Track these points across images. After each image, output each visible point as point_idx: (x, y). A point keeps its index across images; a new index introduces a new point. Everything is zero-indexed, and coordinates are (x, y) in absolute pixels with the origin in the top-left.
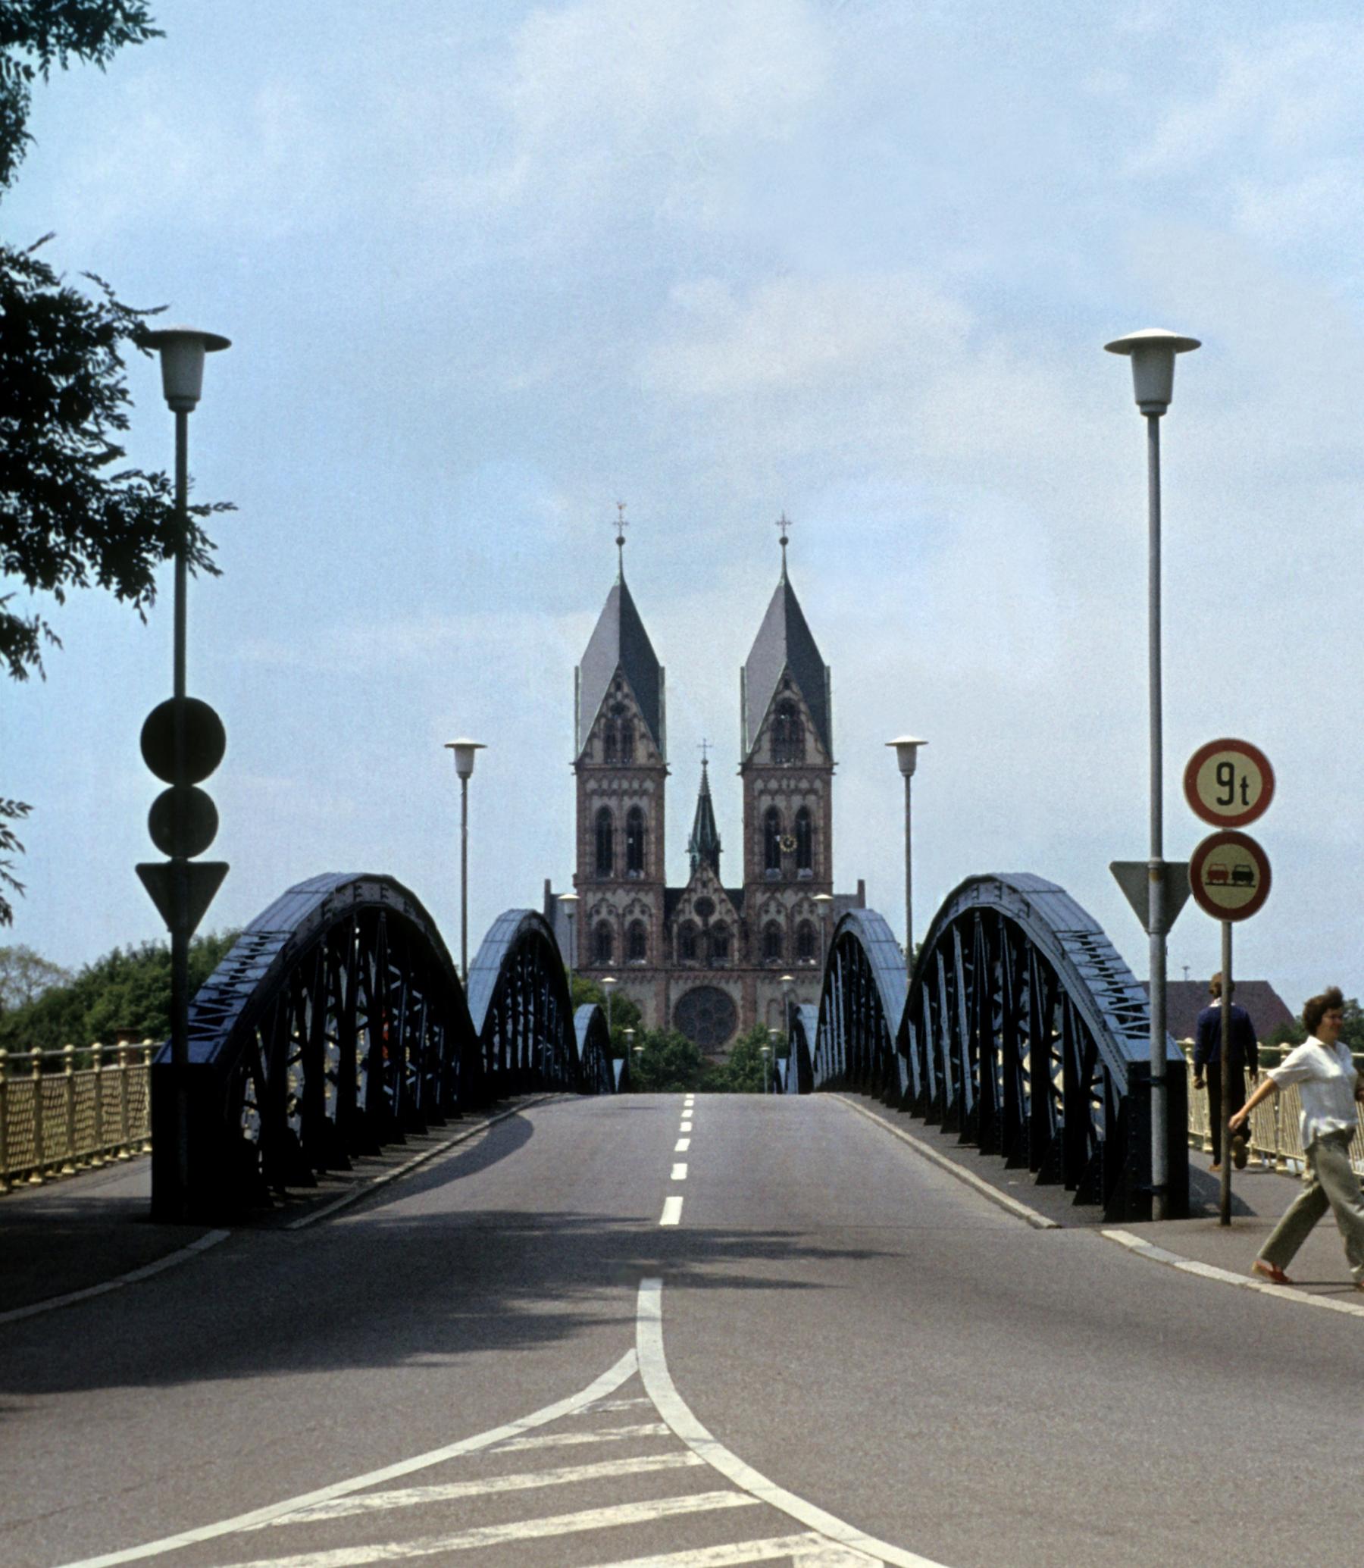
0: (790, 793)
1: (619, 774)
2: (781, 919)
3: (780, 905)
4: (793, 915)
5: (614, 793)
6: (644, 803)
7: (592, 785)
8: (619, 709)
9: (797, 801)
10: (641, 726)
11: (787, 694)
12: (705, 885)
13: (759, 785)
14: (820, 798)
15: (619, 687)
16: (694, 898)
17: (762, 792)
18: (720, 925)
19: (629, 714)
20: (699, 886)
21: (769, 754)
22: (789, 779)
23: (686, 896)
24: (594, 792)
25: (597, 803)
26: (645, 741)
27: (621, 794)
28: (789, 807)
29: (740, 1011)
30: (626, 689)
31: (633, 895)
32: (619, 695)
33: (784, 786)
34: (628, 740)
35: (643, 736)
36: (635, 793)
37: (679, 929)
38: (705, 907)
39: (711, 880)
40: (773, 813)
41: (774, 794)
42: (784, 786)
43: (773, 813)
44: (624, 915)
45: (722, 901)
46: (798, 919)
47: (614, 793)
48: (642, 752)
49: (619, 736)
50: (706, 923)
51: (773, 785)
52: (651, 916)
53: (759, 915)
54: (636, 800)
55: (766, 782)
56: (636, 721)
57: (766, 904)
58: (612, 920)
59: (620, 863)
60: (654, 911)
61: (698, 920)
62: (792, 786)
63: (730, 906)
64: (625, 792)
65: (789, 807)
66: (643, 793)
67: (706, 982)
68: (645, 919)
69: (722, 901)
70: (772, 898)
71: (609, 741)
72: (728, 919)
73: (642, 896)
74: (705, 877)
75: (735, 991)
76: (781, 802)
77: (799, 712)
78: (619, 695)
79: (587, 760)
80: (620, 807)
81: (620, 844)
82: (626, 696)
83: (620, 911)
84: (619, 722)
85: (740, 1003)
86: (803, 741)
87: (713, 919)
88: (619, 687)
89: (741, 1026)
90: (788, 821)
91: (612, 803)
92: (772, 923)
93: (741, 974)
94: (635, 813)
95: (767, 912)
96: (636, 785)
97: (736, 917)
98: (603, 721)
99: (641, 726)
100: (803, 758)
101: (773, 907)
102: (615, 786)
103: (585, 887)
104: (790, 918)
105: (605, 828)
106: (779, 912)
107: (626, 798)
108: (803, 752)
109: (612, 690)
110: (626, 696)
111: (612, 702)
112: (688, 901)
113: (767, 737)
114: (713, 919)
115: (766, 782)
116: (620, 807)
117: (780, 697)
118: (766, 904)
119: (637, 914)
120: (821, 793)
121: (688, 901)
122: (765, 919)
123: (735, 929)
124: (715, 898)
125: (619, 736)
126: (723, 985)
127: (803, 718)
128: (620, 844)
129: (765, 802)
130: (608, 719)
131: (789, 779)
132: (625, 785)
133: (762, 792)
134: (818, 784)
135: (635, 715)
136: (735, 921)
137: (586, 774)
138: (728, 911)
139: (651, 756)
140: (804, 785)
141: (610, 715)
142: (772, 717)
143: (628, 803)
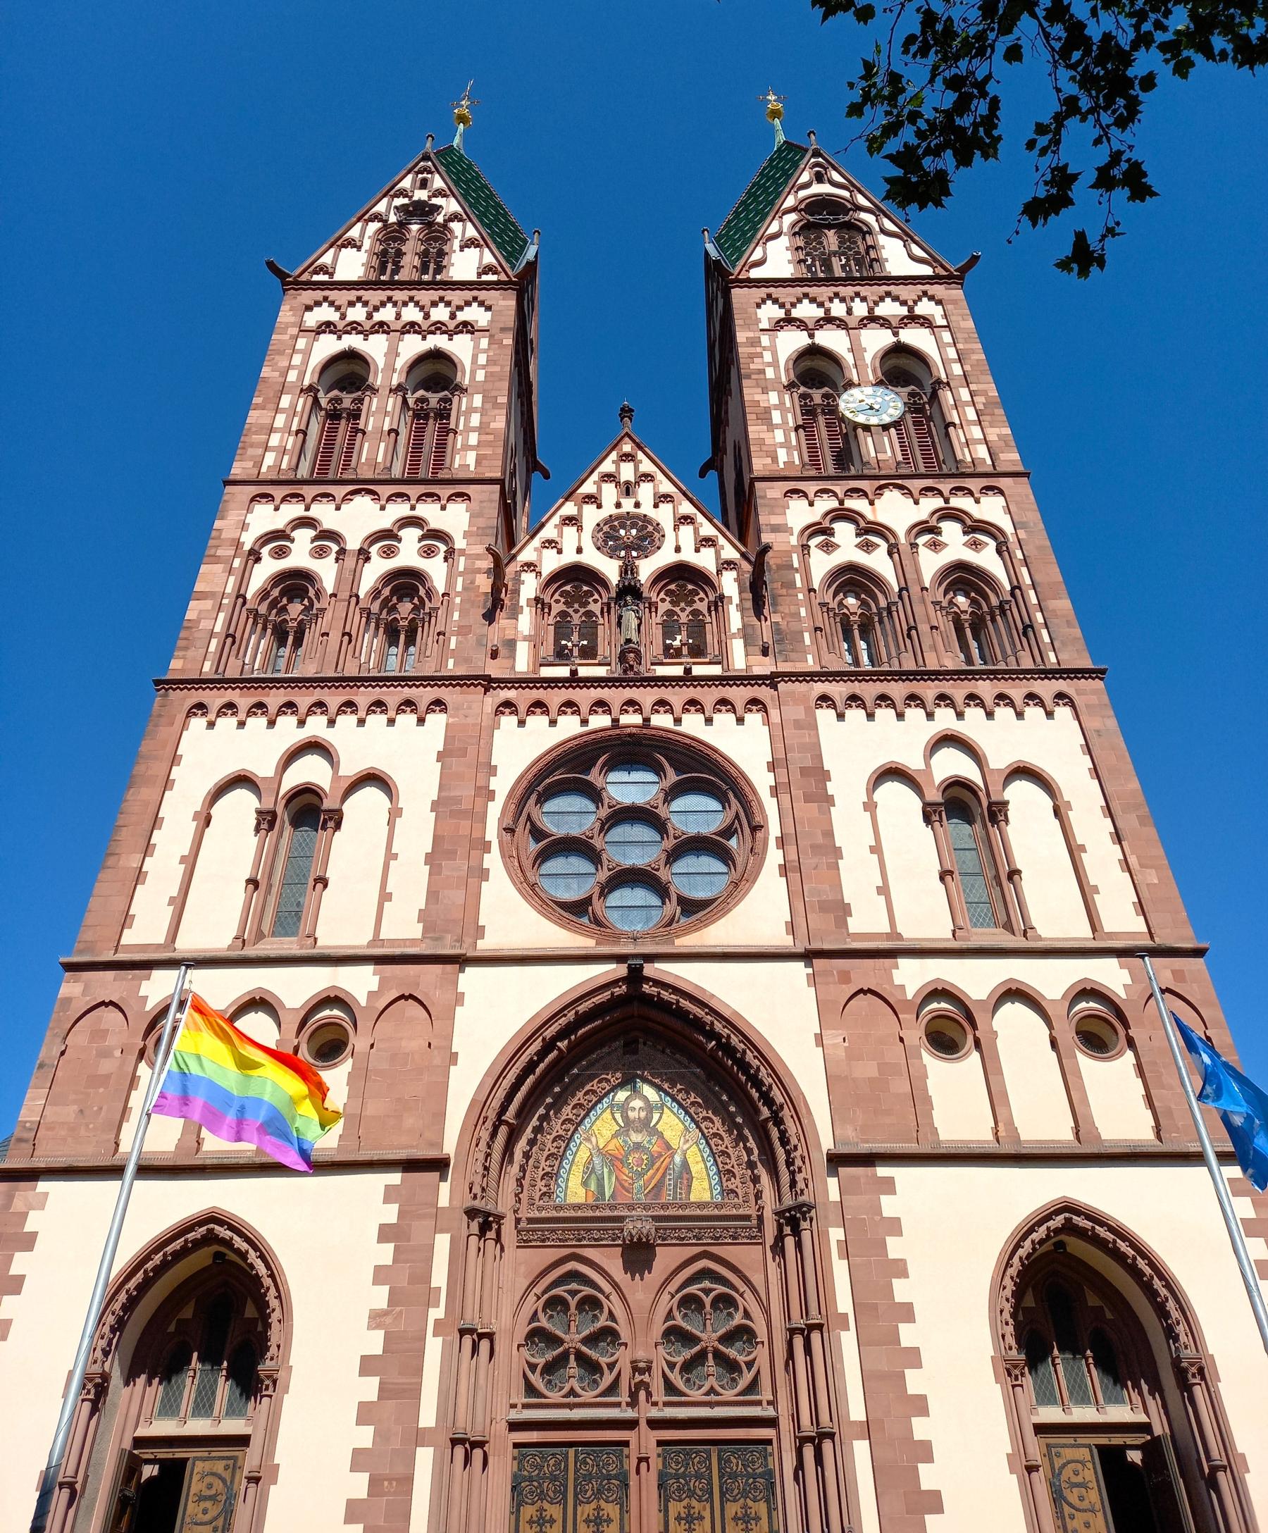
5: (382, 327)
18: (682, 576)
29: (770, 806)
46: (930, 564)
47: (382, 327)
50: (628, 569)
52: (450, 554)
60: (460, 543)
64: (412, 327)
67: (631, 719)
68: (436, 570)
73: (428, 511)
75: (743, 743)
82: (439, 193)
85: (762, 780)
87: (647, 569)
89: (774, 857)
93: (752, 692)
110: (439, 193)
119: (409, 553)
121: (570, 520)
122: (821, 564)
123: (729, 584)
126: (693, 725)
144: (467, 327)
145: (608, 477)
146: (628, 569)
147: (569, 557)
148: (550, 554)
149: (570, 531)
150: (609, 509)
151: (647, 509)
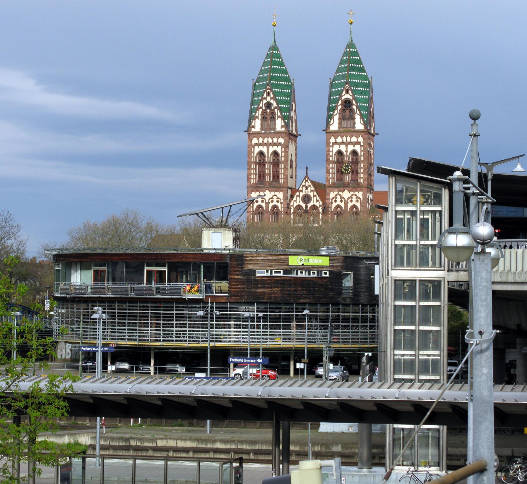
0: (347, 144)
1: (268, 135)
2: (343, 205)
3: (341, 197)
4: (348, 202)
6: (279, 149)
7: (255, 141)
8: (269, 105)
9: (351, 148)
10: (278, 113)
11: (347, 96)
12: (307, 188)
13: (333, 140)
14: (361, 146)
15: (268, 94)
16: (302, 194)
17: (335, 143)
18: (314, 207)
19: (273, 108)
20: (304, 188)
21: (337, 126)
22: (347, 137)
23: (298, 193)
24: (256, 144)
25: (257, 149)
26: (280, 119)
27: (268, 145)
28: (347, 151)
30: (272, 95)
31: (273, 193)
32: (268, 98)
33: (345, 141)
34: (273, 118)
35: (279, 117)
36: (273, 144)
37: (294, 210)
38: (307, 199)
39: (310, 186)
40: (340, 153)
41: (339, 144)
42: (345, 141)
43: (340, 153)
44: (269, 203)
45: (314, 196)
46: (350, 205)
48: (279, 125)
49: (268, 117)
50: (306, 207)
51: (339, 140)
52: (281, 203)
53: (332, 203)
54: (275, 148)
55: (336, 138)
56: (276, 110)
57: (335, 197)
58: (264, 205)
59: (269, 179)
60: (282, 201)
61: (303, 205)
62: (349, 141)
63: (318, 198)
65: (347, 151)
68: (279, 205)
69: (314, 196)
70: (338, 194)
71: (264, 119)
72: (317, 204)
73: (277, 193)
74: (307, 185)
76: (343, 148)
77: (353, 104)
78: (268, 98)
79: (253, 129)
80: (268, 152)
81: (269, 169)
82: (271, 98)
83: (267, 201)
84: (268, 111)
86: (354, 119)
87: (309, 205)
88: (268, 94)
90: (348, 158)
91: (264, 149)
92: (338, 206)
94: (275, 153)
95: (336, 201)
96: (275, 140)
97: (321, 204)
98: (261, 110)
99: (278, 113)
100: (354, 126)
102: (266, 141)
103: (251, 189)
104: (346, 204)
105: (262, 161)
106: (341, 201)
107: (271, 147)
108: (354, 123)
109: (265, 95)
111: (265, 101)
112: (299, 196)
113: (336, 118)
114: (309, 205)
115: (336, 138)
116: (268, 152)
117: (343, 98)
118: (335, 197)
120: (362, 144)
121: (299, 196)
122: (334, 205)
124: (312, 194)
125: (268, 117)
127: (354, 107)
128: (269, 169)
129: (336, 148)
130: (263, 110)
131: (347, 137)
132: (270, 141)
133: (335, 143)
134: (361, 139)
135: (275, 108)
136: (320, 206)
137: (252, 135)
138: (317, 201)
139: (282, 126)
140: (354, 139)
141: (264, 108)
142: (340, 107)
143: (272, 149)
144: (280, 144)
145: (303, 186)
146: (306, 207)
147: (298, 203)
148: (295, 202)
149: (298, 197)
150: (304, 193)
151: (309, 193)
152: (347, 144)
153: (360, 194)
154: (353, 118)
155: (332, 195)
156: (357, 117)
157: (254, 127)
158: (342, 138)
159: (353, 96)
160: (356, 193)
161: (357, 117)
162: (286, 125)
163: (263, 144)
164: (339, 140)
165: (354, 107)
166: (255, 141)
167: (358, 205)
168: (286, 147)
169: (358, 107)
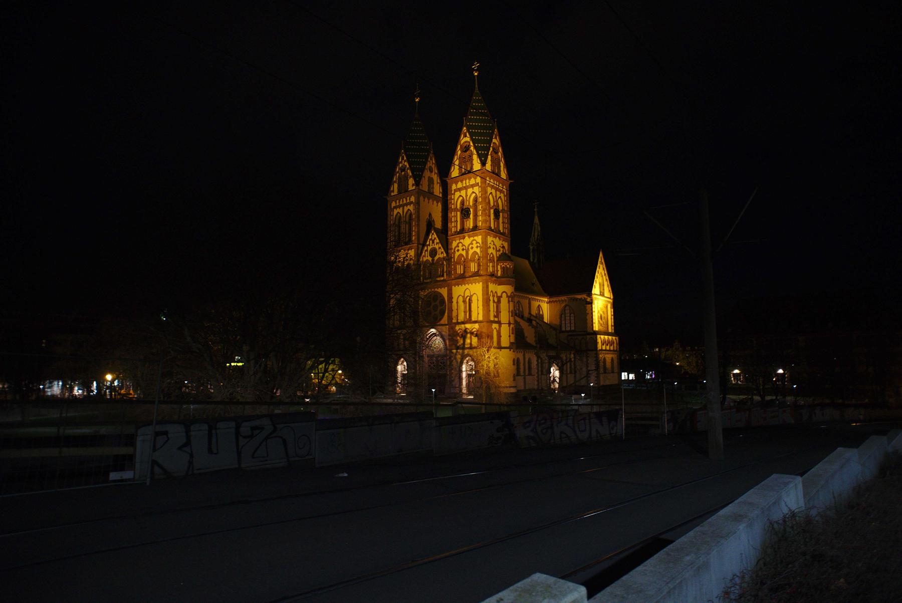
0: (466, 188)
2: (464, 253)
13: (454, 187)
15: (403, 159)
16: (429, 248)
36: (407, 205)
38: (433, 253)
41: (460, 190)
50: (433, 260)
51: (460, 185)
66: (411, 203)
88: (403, 159)
100: (472, 168)
101: (460, 248)
108: (472, 165)
114: (436, 258)
124: (437, 247)
134: (479, 180)
140: (472, 181)
142: (459, 152)
144: (411, 203)
152: (466, 188)
153: (479, 239)
154: (471, 160)
155: (454, 244)
156: (475, 157)
157: (393, 191)
158: (462, 181)
159: (472, 139)
160: (476, 238)
161: (475, 157)
162: (417, 183)
163: (399, 207)
164: (460, 185)
165: (472, 148)
166: (393, 204)
167: (478, 250)
168: (417, 204)
169: (475, 147)
